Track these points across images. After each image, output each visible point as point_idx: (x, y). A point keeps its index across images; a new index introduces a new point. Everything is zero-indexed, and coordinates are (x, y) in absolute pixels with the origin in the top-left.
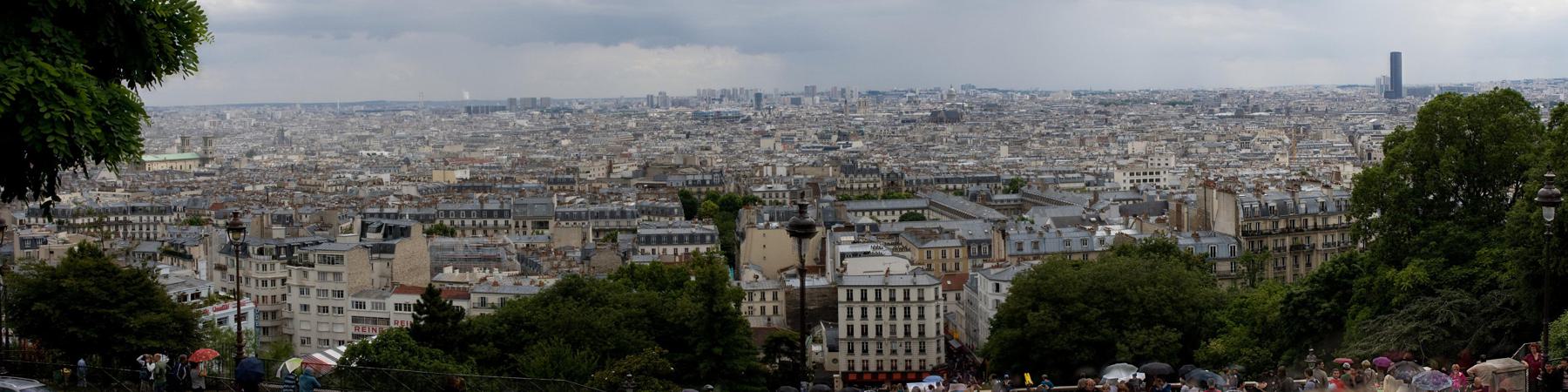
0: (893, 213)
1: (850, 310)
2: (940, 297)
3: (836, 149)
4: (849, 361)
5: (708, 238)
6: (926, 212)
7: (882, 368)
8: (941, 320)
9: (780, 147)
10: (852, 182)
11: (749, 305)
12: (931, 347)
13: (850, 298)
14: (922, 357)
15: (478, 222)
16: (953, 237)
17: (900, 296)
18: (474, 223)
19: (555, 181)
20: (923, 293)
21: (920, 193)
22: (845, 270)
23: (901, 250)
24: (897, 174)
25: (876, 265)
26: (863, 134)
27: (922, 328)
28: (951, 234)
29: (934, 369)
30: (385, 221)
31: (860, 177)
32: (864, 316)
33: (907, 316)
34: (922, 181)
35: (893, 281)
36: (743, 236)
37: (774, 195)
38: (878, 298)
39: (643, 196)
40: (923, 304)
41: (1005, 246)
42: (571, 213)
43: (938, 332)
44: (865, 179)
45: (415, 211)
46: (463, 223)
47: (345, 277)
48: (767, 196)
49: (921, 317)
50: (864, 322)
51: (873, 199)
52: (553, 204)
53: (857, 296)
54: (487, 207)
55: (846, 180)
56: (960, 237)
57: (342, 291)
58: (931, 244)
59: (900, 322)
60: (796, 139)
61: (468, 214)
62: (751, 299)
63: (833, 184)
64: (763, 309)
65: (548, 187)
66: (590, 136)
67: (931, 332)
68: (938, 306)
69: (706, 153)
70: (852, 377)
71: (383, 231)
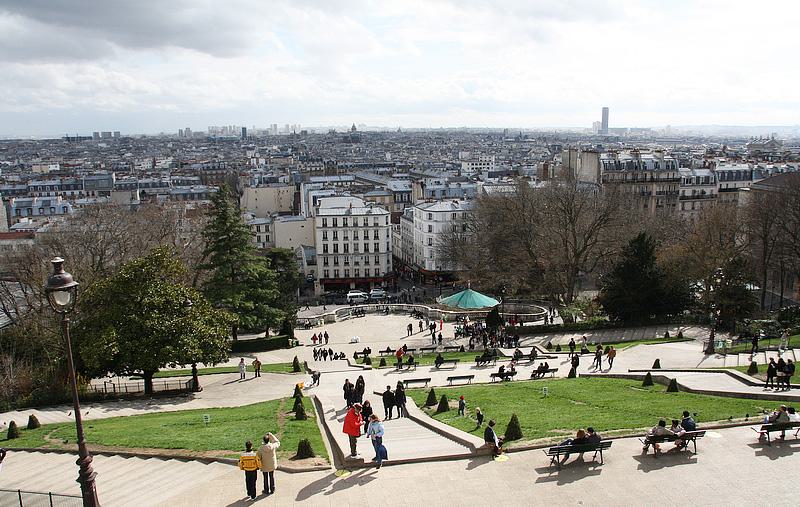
8: (390, 240)
12: (383, 260)
13: (325, 225)
14: (377, 267)
21: (348, 173)
23: (357, 193)
27: (376, 245)
32: (335, 238)
33: (366, 238)
49: (376, 237)
50: (336, 242)
53: (330, 223)
54: (67, 183)
55: (302, 166)
61: (52, 188)
67: (383, 249)
70: (328, 281)
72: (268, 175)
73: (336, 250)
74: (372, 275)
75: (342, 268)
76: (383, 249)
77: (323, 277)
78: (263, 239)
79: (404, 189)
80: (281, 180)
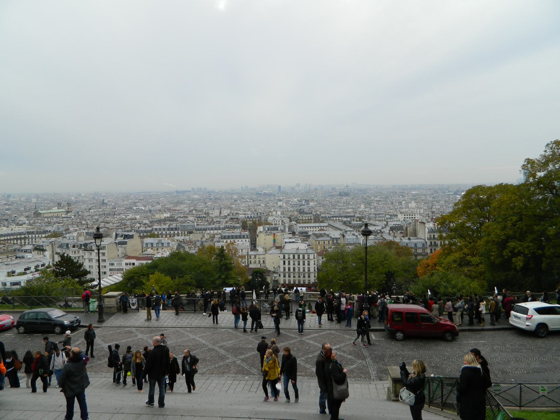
0: (316, 228)
1: (284, 262)
2: (316, 257)
3: (304, 205)
5: (246, 236)
6: (327, 227)
7: (295, 282)
8: (316, 266)
9: (284, 205)
10: (302, 217)
11: (255, 260)
13: (284, 258)
14: (309, 279)
15: (168, 232)
16: (328, 237)
17: (301, 257)
18: (166, 232)
19: (199, 217)
22: (284, 247)
23: (305, 241)
24: (318, 215)
25: (294, 246)
27: (309, 268)
28: (328, 235)
29: (313, 283)
30: (124, 233)
31: (305, 215)
32: (289, 264)
33: (304, 264)
35: (300, 252)
37: (275, 221)
38: (294, 258)
39: (228, 222)
40: (309, 260)
42: (201, 228)
43: (315, 270)
44: (307, 216)
45: (142, 229)
46: (162, 233)
47: (106, 254)
48: (273, 221)
49: (309, 264)
50: (289, 266)
51: (311, 223)
52: (194, 225)
53: (287, 257)
54: (171, 227)
55: (300, 216)
56: (330, 237)
58: (320, 239)
59: (301, 266)
60: (290, 202)
61: (164, 229)
62: (255, 258)
63: (296, 218)
64: (259, 261)
65: (197, 219)
67: (312, 270)
69: (259, 207)
71: (123, 237)
72: (274, 226)
73: (289, 269)
74: (307, 283)
75: (292, 279)
76: (312, 270)
78: (262, 262)
79: (339, 237)
80: (279, 229)
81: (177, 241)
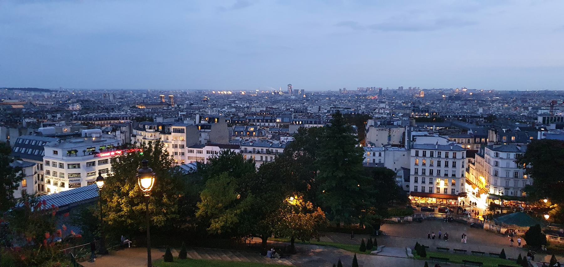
4: (415, 186)
9: (387, 107)
15: (262, 124)
17: (443, 154)
20: (455, 155)
23: (444, 135)
26: (421, 103)
33: (447, 165)
34: (448, 116)
36: (368, 131)
40: (456, 160)
41: (496, 137)
44: (423, 114)
49: (454, 166)
52: (292, 118)
57: (184, 145)
66: (317, 102)
68: (463, 162)
73: (424, 173)
77: (413, 190)
80: (395, 123)
81: (272, 132)
